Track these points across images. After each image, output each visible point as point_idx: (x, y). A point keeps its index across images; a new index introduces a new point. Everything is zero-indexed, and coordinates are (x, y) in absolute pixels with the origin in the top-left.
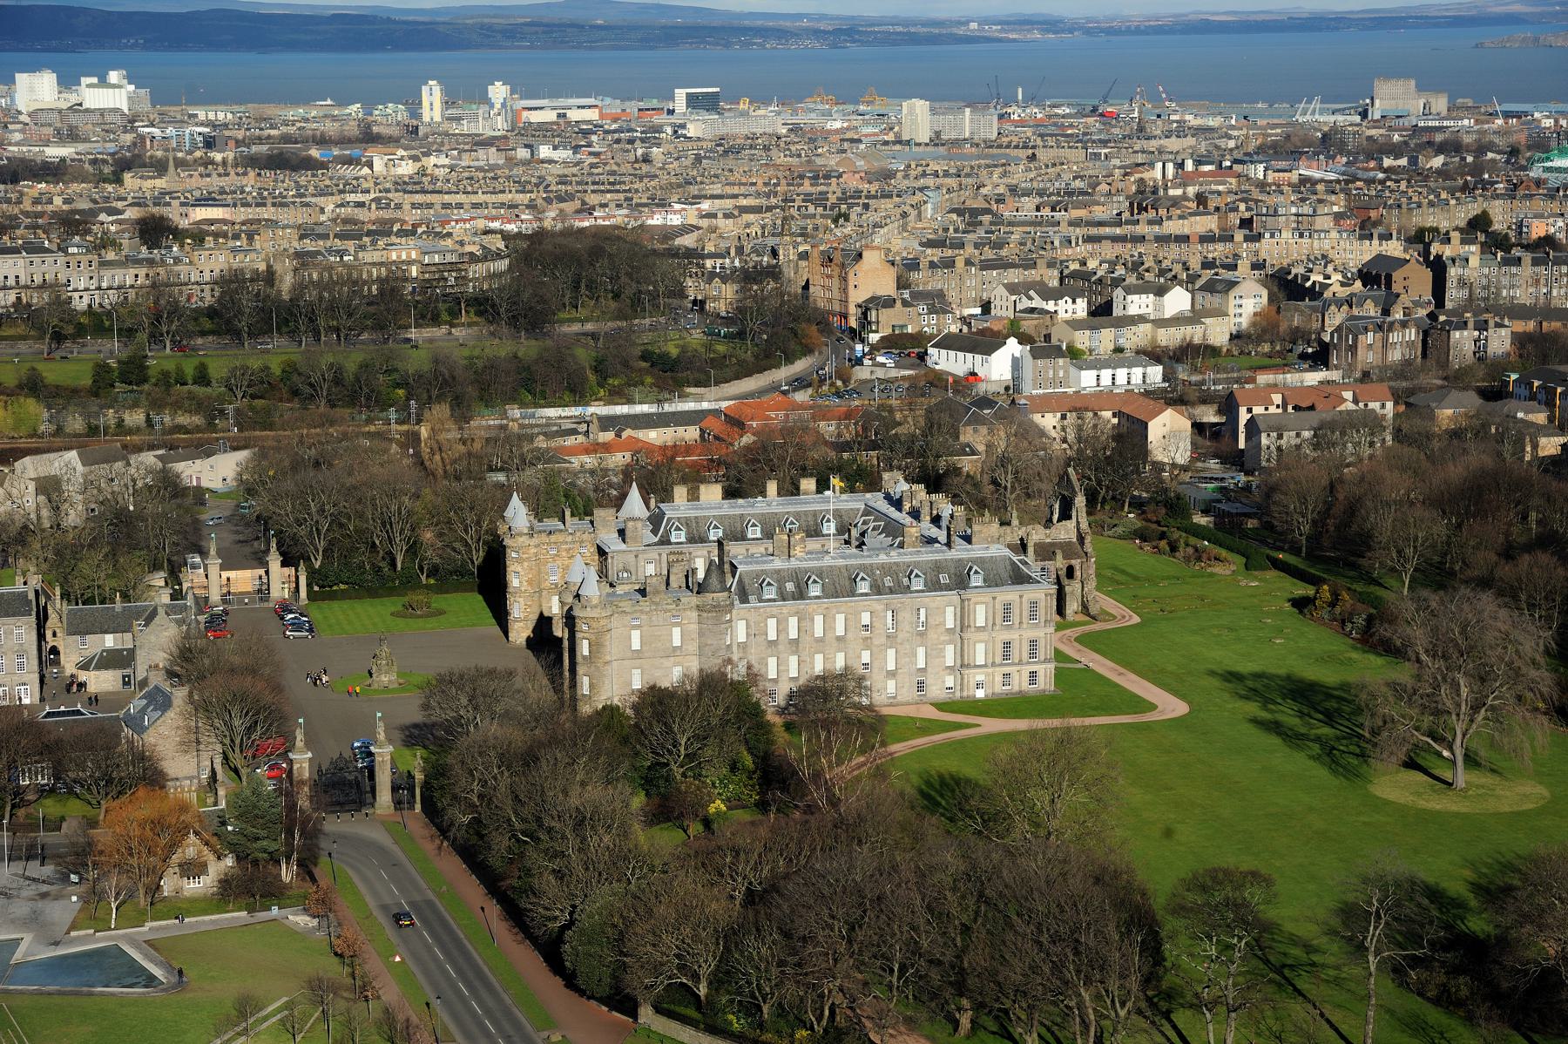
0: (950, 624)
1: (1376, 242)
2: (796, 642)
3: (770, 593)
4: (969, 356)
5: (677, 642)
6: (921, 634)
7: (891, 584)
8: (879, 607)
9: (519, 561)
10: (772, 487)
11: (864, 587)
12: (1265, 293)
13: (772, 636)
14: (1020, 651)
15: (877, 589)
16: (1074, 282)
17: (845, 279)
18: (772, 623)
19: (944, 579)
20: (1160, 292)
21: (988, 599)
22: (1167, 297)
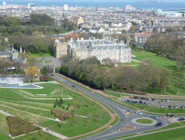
0: (118, 53)
1: (140, 20)
2: (99, 55)
3: (96, 49)
4: (96, 30)
5: (85, 55)
6: (115, 54)
7: (112, 48)
8: (110, 51)
9: (58, 47)
10: (90, 38)
11: (108, 48)
12: (131, 24)
13: (97, 54)
14: (127, 57)
15: (109, 48)
16: (107, 22)
17: (77, 21)
18: (97, 53)
19: (117, 48)
20: (118, 24)
21: (123, 50)
22: (119, 24)
